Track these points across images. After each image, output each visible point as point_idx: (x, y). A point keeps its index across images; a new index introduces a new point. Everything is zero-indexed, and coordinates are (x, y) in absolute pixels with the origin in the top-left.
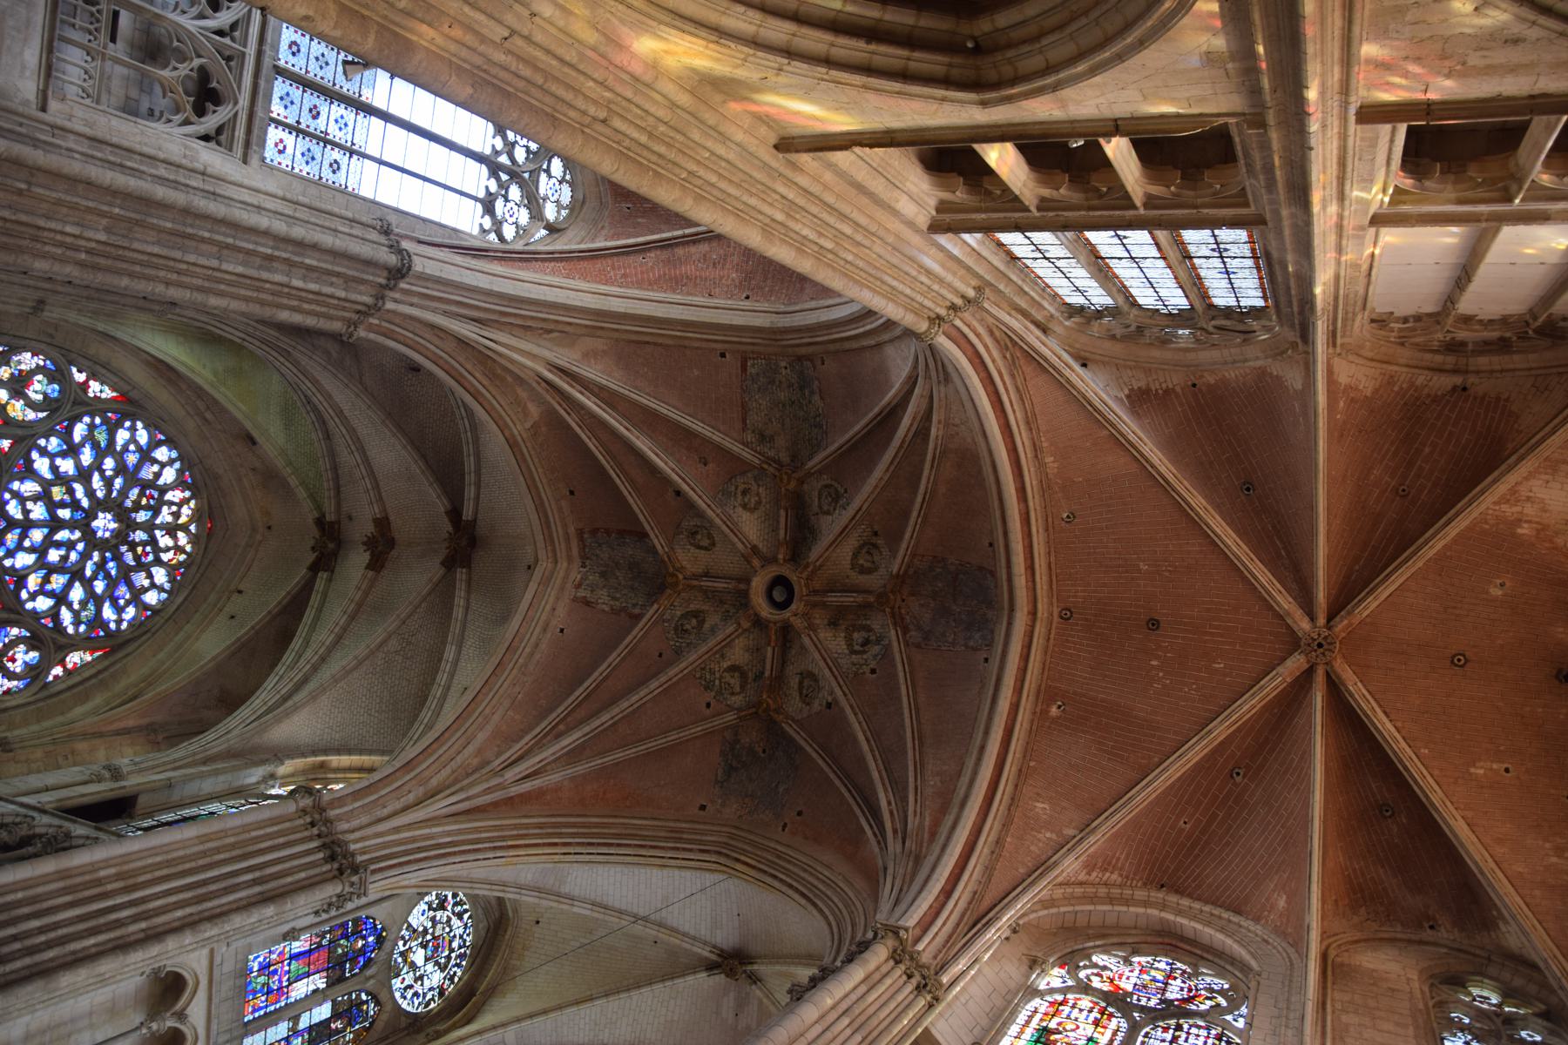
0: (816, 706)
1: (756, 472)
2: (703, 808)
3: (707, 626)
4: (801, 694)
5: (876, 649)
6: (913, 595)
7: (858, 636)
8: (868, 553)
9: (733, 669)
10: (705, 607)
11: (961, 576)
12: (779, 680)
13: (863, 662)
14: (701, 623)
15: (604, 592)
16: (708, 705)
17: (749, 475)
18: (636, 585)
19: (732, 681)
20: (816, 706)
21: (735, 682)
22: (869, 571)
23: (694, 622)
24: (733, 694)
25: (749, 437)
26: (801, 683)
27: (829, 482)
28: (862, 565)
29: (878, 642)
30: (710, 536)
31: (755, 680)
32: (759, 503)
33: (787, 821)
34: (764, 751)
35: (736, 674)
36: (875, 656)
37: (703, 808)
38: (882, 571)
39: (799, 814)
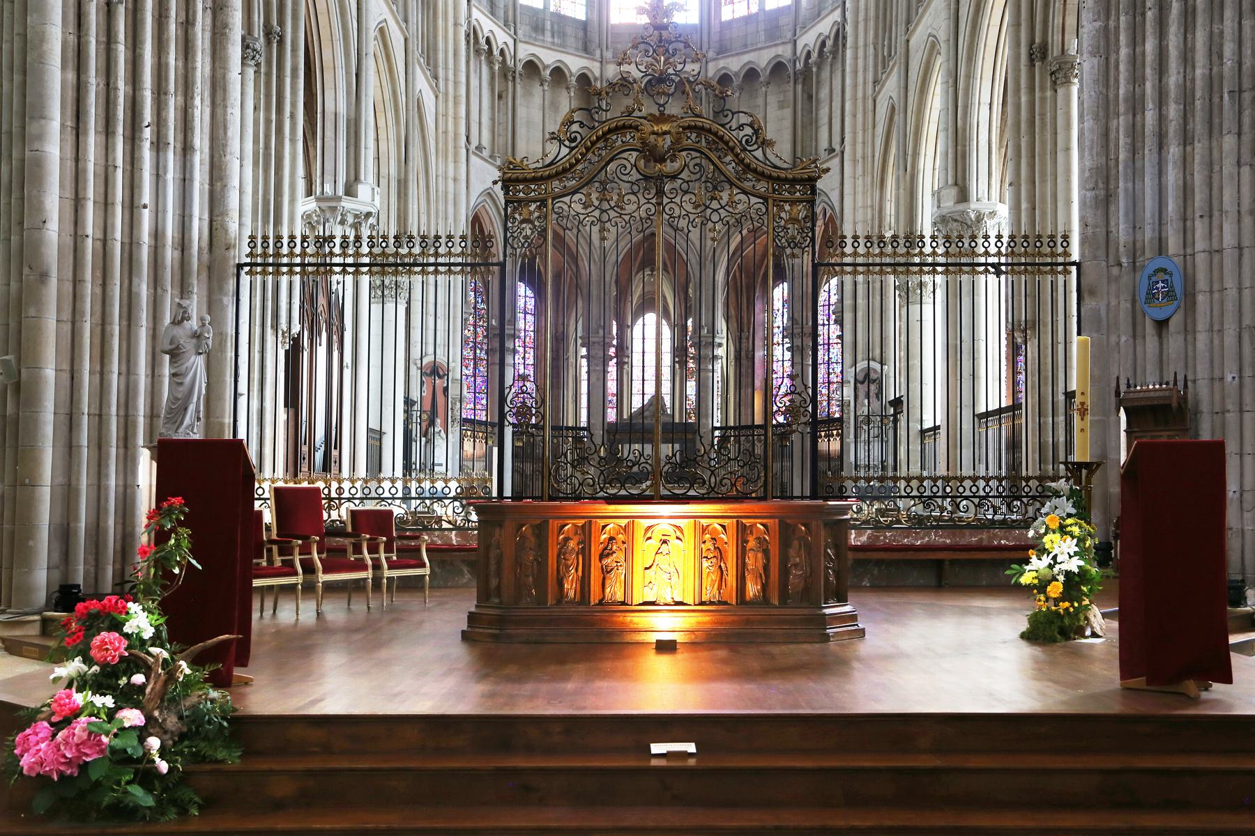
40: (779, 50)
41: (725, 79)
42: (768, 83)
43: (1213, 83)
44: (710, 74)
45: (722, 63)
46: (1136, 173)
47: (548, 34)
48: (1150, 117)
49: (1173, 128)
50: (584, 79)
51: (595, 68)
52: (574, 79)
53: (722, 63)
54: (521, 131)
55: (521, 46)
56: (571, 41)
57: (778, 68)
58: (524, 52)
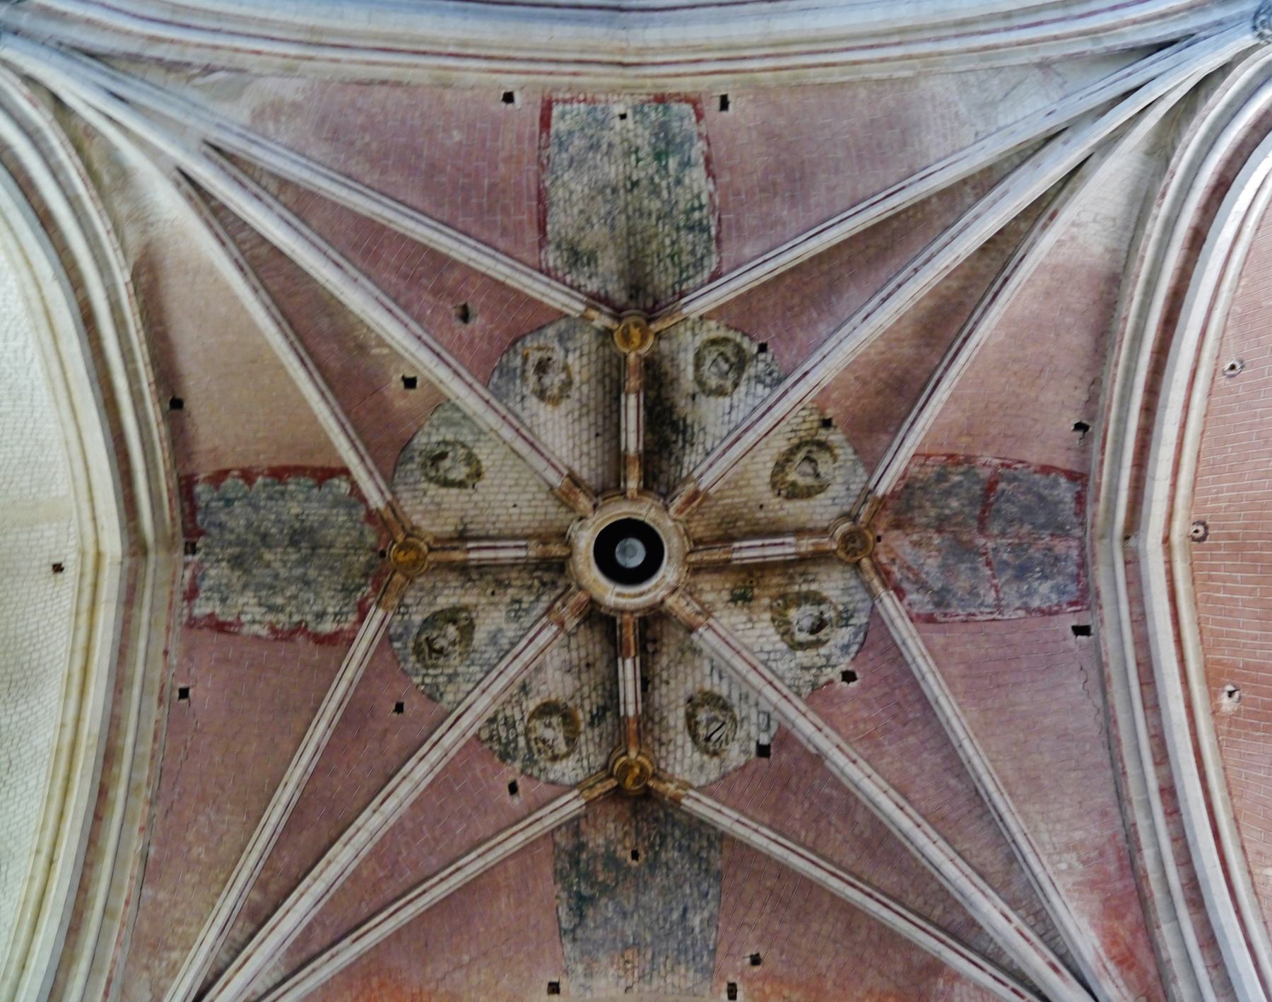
0: (735, 755)
1: (563, 325)
3: (480, 636)
4: (694, 737)
6: (897, 525)
7: (801, 616)
8: (808, 459)
9: (546, 710)
10: (468, 600)
11: (1002, 485)
12: (649, 718)
13: (823, 662)
14: (467, 631)
15: (249, 598)
16: (513, 788)
17: (550, 331)
18: (312, 573)
19: (549, 734)
20: (735, 755)
21: (554, 733)
22: (809, 493)
23: (452, 630)
24: (555, 758)
25: (552, 258)
26: (691, 720)
27: (722, 333)
28: (794, 484)
29: (844, 619)
30: (471, 459)
31: (591, 724)
32: (568, 383)
33: (731, 979)
34: (635, 855)
35: (556, 720)
36: (845, 648)
38: (836, 490)
39: (756, 960)
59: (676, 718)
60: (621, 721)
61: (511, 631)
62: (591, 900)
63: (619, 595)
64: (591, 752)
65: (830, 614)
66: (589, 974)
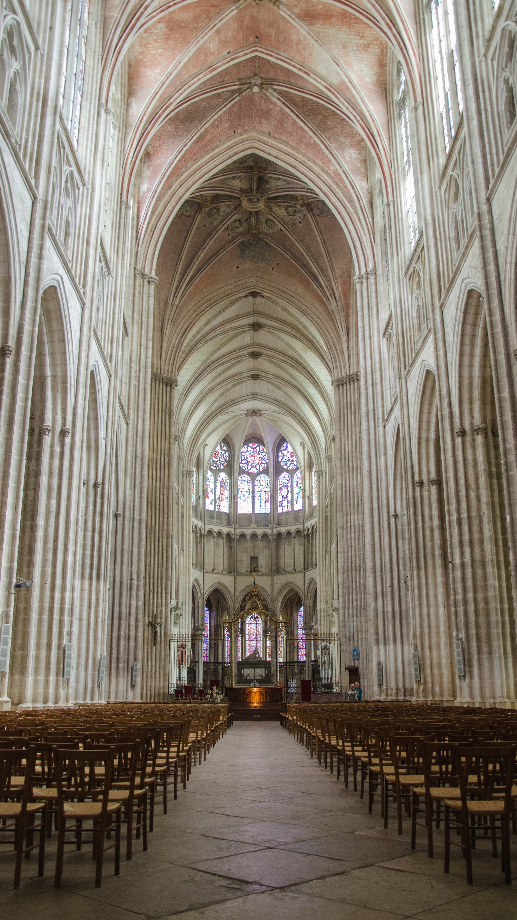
0: (275, 230)
2: (238, 267)
3: (221, 211)
5: (300, 215)
14: (218, 210)
20: (275, 230)
21: (237, 224)
23: (215, 211)
29: (300, 212)
36: (300, 217)
37: (238, 267)
39: (278, 264)
40: (299, 526)
41: (279, 535)
42: (295, 537)
43: (361, 606)
44: (274, 532)
45: (278, 529)
46: (349, 622)
47: (215, 519)
48: (351, 611)
49: (355, 614)
50: (229, 535)
51: (232, 531)
52: (224, 536)
53: (278, 529)
54: (206, 554)
55: (206, 526)
56: (224, 521)
57: (298, 532)
58: (208, 527)
59: (264, 221)
60: (251, 224)
61: (228, 210)
62: (245, 250)
63: (252, 208)
64: (245, 226)
65: (297, 210)
66: (245, 263)
